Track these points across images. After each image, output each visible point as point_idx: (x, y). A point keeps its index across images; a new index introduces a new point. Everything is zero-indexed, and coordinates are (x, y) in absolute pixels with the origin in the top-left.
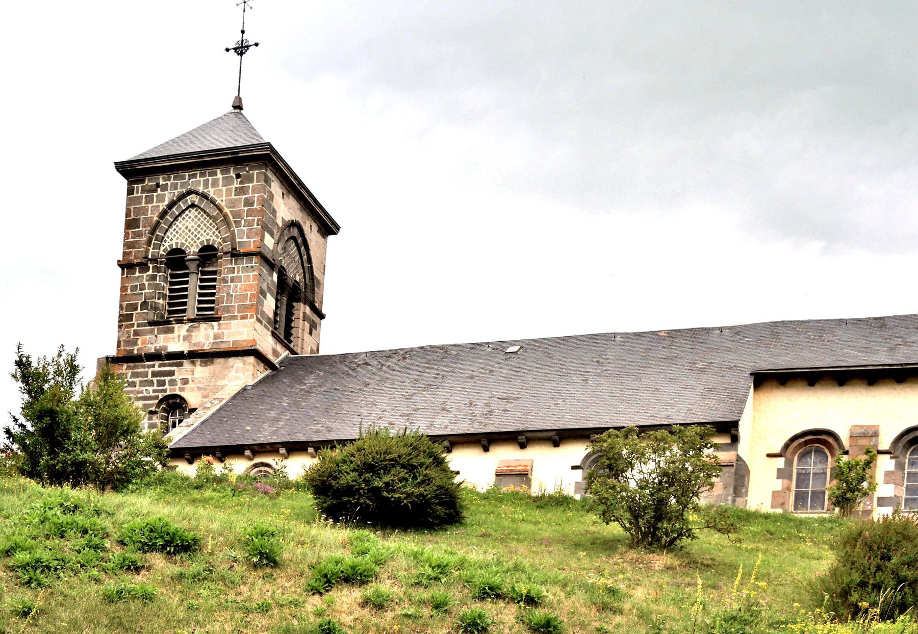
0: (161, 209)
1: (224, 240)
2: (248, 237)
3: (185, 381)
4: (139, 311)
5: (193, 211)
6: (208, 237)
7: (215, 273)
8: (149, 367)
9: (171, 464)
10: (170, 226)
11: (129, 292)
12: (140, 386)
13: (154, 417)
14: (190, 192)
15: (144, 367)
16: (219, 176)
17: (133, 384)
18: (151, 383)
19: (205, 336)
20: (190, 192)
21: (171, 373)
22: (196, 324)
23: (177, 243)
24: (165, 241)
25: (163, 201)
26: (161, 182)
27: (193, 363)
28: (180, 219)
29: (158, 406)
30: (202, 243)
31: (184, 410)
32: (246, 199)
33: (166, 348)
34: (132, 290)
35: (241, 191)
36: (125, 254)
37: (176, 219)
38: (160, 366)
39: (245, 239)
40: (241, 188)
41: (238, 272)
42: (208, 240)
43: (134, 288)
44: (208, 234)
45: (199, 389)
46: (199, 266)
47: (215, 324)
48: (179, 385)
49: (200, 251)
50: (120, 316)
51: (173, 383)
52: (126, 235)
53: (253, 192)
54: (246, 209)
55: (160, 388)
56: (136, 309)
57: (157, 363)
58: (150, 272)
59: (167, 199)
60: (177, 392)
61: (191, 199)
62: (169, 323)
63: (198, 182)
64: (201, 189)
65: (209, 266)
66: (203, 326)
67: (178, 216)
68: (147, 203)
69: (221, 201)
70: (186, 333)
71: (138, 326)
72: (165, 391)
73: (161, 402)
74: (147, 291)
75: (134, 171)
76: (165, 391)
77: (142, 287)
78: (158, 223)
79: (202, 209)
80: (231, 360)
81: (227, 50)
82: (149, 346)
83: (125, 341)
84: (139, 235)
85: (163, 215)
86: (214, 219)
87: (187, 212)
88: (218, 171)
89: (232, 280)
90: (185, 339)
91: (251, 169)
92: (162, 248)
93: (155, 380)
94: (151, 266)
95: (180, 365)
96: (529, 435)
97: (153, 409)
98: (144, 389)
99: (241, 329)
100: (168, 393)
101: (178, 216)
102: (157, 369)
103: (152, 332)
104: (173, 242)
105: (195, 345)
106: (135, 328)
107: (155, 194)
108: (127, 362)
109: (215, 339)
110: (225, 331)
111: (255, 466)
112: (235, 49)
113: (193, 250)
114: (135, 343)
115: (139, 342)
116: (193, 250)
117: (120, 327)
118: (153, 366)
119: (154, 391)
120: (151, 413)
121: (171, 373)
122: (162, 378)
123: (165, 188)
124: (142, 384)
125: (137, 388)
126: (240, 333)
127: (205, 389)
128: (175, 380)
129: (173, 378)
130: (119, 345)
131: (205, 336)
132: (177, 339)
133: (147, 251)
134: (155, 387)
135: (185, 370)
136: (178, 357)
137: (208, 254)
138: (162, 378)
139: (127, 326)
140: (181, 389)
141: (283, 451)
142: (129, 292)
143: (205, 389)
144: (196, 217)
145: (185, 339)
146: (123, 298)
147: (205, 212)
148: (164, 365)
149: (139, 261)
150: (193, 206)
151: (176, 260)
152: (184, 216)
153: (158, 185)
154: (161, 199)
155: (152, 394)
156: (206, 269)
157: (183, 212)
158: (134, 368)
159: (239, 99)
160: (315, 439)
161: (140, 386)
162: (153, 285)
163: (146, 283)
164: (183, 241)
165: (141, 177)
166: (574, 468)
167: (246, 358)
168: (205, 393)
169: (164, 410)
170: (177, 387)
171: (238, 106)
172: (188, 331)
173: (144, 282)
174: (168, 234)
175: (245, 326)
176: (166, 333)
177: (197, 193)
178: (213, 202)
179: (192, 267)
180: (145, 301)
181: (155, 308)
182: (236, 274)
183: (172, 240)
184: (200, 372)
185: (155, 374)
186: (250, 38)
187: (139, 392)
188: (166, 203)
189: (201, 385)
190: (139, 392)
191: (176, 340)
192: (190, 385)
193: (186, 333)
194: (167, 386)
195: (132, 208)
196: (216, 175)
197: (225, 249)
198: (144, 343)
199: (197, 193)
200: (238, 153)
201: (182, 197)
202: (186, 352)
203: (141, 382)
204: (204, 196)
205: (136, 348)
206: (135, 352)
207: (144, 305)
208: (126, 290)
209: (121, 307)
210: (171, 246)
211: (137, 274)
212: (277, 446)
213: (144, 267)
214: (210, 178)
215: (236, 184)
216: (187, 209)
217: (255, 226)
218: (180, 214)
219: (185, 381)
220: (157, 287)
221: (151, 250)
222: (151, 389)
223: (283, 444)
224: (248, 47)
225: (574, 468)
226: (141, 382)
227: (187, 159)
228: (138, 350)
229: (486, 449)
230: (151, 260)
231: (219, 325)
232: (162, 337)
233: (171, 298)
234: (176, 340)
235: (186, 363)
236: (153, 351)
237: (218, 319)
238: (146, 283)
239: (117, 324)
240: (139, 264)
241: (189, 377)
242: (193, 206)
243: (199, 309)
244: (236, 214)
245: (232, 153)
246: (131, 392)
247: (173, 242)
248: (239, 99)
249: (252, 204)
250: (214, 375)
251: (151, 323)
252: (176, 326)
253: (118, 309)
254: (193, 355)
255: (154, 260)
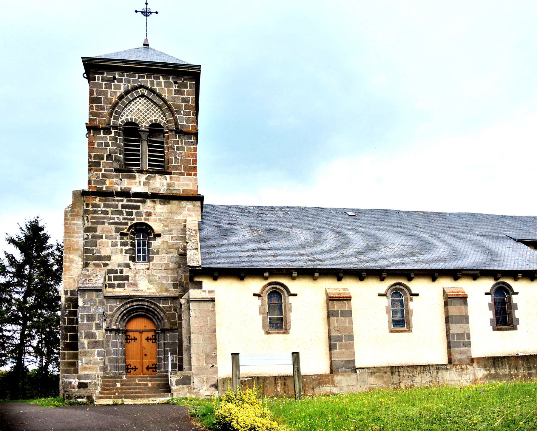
0: (118, 94)
1: (168, 122)
2: (187, 122)
3: (149, 214)
4: (105, 160)
5: (143, 99)
6: (156, 118)
7: (162, 143)
8: (119, 201)
9: (197, 279)
10: (126, 106)
11: (96, 146)
12: (112, 214)
13: (125, 238)
14: (141, 87)
15: (114, 201)
16: (161, 80)
17: (106, 213)
18: (121, 213)
19: (160, 184)
20: (141, 87)
21: (138, 207)
22: (153, 175)
23: (131, 119)
24: (122, 116)
25: (120, 89)
26: (117, 77)
27: (154, 202)
28: (133, 103)
29: (128, 230)
30: (151, 121)
31: (149, 234)
32: (182, 98)
33: (130, 189)
34: (98, 145)
35: (178, 92)
36: (90, 120)
37: (130, 102)
38: (128, 201)
39: (185, 123)
40: (178, 91)
41: (182, 144)
42: (156, 120)
43: (100, 144)
44: (155, 116)
45: (161, 220)
46: (149, 136)
47: (168, 176)
48: (144, 216)
49: (150, 126)
50: (89, 162)
51: (139, 214)
52: (91, 108)
53: (188, 94)
54: (184, 104)
55: (129, 217)
56: (103, 159)
57: (125, 199)
58: (113, 135)
59: (122, 88)
60: (143, 221)
61: (141, 91)
62: (132, 171)
63: (147, 81)
64: (149, 85)
65: (155, 137)
66: (158, 177)
67: (132, 101)
68: (106, 88)
69: (166, 95)
70: (145, 181)
71: (105, 171)
72: (133, 219)
73: (130, 228)
74: (110, 147)
75: (93, 67)
76: (133, 219)
77: (107, 144)
78: (117, 103)
79: (150, 99)
80: (184, 203)
81: (136, 11)
82: (116, 186)
83: (95, 181)
84: (102, 108)
85: (121, 97)
86: (160, 107)
87: (138, 99)
88: (161, 77)
89: (178, 149)
90: (144, 184)
91: (185, 79)
92: (120, 120)
93: (124, 211)
94: (113, 131)
95: (144, 202)
96: (464, 272)
97: (125, 231)
98: (116, 216)
99: (188, 182)
100: (135, 221)
101: (132, 101)
102: (125, 203)
103: (117, 176)
104: (129, 117)
105: (153, 189)
106: (103, 172)
107: (113, 84)
108: (99, 196)
109: (168, 187)
110: (176, 183)
111: (270, 284)
112: (142, 12)
113: (144, 125)
114: (104, 183)
115: (107, 182)
116: (144, 125)
117: (90, 170)
118: (122, 201)
119: (124, 219)
120: (122, 234)
121: (138, 207)
122: (130, 210)
123: (120, 81)
124: (113, 213)
125: (109, 215)
126: (188, 185)
127: (165, 221)
128: (140, 212)
129: (139, 210)
130: (89, 182)
131: (160, 184)
132: (138, 183)
133: (110, 120)
134: (125, 216)
135: (147, 206)
136: (142, 196)
137: (155, 129)
138: (130, 210)
139: (96, 170)
140: (147, 220)
141: (295, 274)
142: (96, 146)
143: (165, 221)
144: (145, 103)
145: (144, 184)
146: (91, 150)
147: (152, 101)
148: (131, 201)
149: (103, 126)
150: (143, 96)
151: (131, 130)
152: (136, 101)
153: (114, 78)
154: (118, 87)
155: (122, 220)
156: (152, 139)
157: (135, 98)
158: (106, 200)
159: (146, 40)
160: (319, 267)
161: (112, 214)
162: (111, 142)
163: (110, 142)
164: (137, 118)
165: (100, 71)
166: (486, 294)
167: (195, 202)
168: (165, 224)
169: (133, 233)
170: (143, 218)
171: (146, 45)
172: (146, 179)
173: (108, 141)
174: (124, 111)
175: (190, 180)
176: (128, 178)
177: (146, 88)
178: (159, 96)
179: (144, 136)
180: (110, 155)
181: (118, 160)
182: (180, 145)
183: (127, 116)
184: (160, 208)
185: (123, 207)
186: (152, 7)
187: (111, 219)
188: (122, 90)
189: (162, 218)
190: (111, 219)
191: (138, 184)
192: (153, 217)
193: (145, 181)
194: (134, 216)
195: (95, 90)
196: (159, 79)
197: (170, 128)
198: (111, 183)
199: (146, 88)
200: (178, 68)
201: (135, 89)
202: (149, 193)
203: (112, 211)
204: (152, 91)
205: (104, 187)
206: (104, 189)
207: (109, 157)
208: (94, 145)
209: (90, 156)
210: (127, 119)
211: (102, 135)
212: (292, 271)
213: (107, 131)
214: (155, 81)
215: (175, 87)
216: (138, 97)
217: (192, 116)
218: (133, 100)
219: (149, 214)
220: (119, 146)
221: (112, 120)
222: (121, 217)
223: (296, 270)
224: (151, 13)
225: (486, 294)
226: (112, 211)
227: (140, 65)
228: (106, 188)
229: (434, 280)
230: (112, 126)
231: (171, 177)
232: (126, 181)
233: (126, 155)
234: (138, 184)
235: (149, 202)
236: (119, 190)
237: (170, 173)
238: (110, 142)
239: (87, 168)
240: (102, 128)
241: (152, 211)
242: (143, 96)
243: (150, 165)
244: (178, 107)
245: (173, 67)
246: (104, 218)
247: (129, 117)
248: (146, 40)
249: (188, 102)
250: (171, 211)
251: (116, 170)
252: (137, 175)
253: (87, 158)
254: (155, 197)
255: (115, 127)
